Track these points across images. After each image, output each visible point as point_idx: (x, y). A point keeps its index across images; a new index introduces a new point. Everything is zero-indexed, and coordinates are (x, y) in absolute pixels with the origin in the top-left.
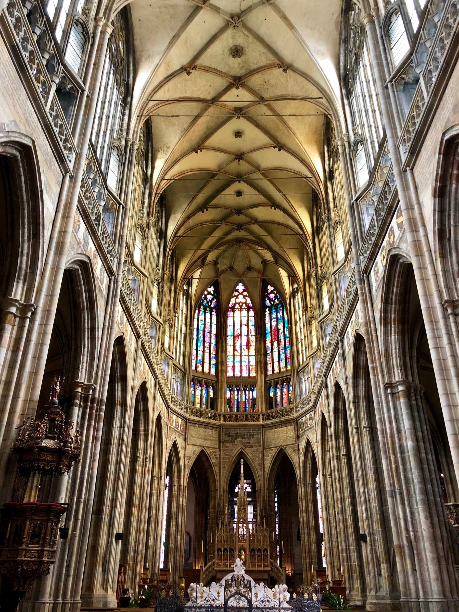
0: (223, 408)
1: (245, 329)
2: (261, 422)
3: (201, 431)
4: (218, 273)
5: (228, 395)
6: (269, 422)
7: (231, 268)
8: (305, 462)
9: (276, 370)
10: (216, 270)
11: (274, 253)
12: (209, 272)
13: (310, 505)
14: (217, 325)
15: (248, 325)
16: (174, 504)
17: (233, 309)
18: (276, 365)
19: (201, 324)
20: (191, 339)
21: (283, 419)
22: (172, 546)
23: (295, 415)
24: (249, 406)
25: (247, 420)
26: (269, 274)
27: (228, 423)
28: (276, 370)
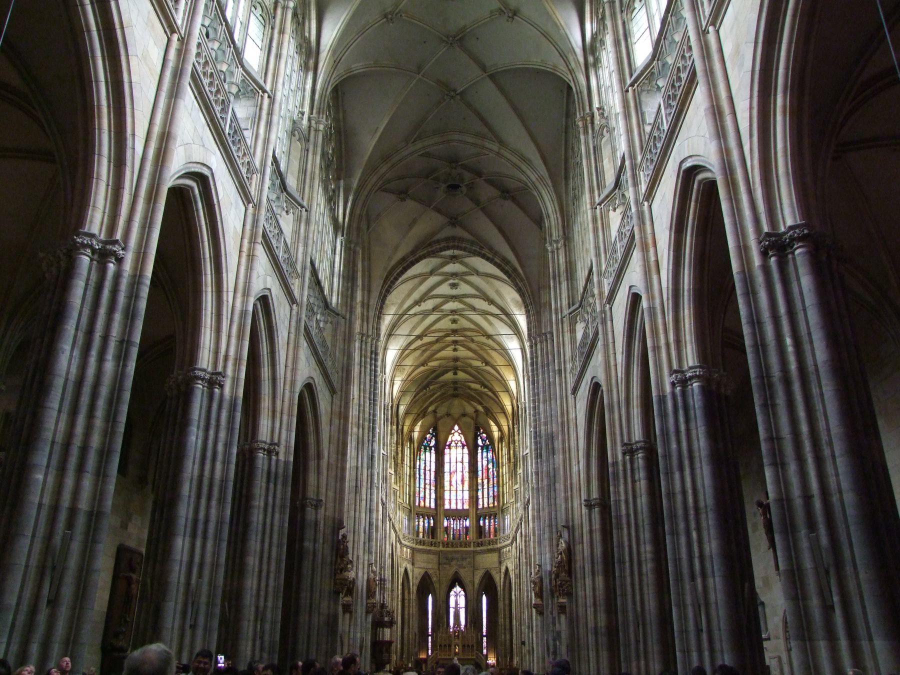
0: (442, 536)
1: (459, 465)
2: (472, 549)
3: (425, 556)
4: (437, 420)
5: (446, 524)
6: (478, 549)
7: (448, 415)
8: (505, 582)
9: (486, 505)
10: (435, 417)
11: (483, 407)
12: (429, 419)
13: (507, 613)
14: (436, 462)
15: (462, 462)
16: (406, 612)
17: (449, 446)
18: (486, 500)
19: (422, 462)
20: (415, 480)
21: (490, 547)
22: (406, 642)
23: (499, 545)
24: (463, 532)
25: (461, 546)
26: (482, 418)
27: (445, 549)
28: (486, 505)
